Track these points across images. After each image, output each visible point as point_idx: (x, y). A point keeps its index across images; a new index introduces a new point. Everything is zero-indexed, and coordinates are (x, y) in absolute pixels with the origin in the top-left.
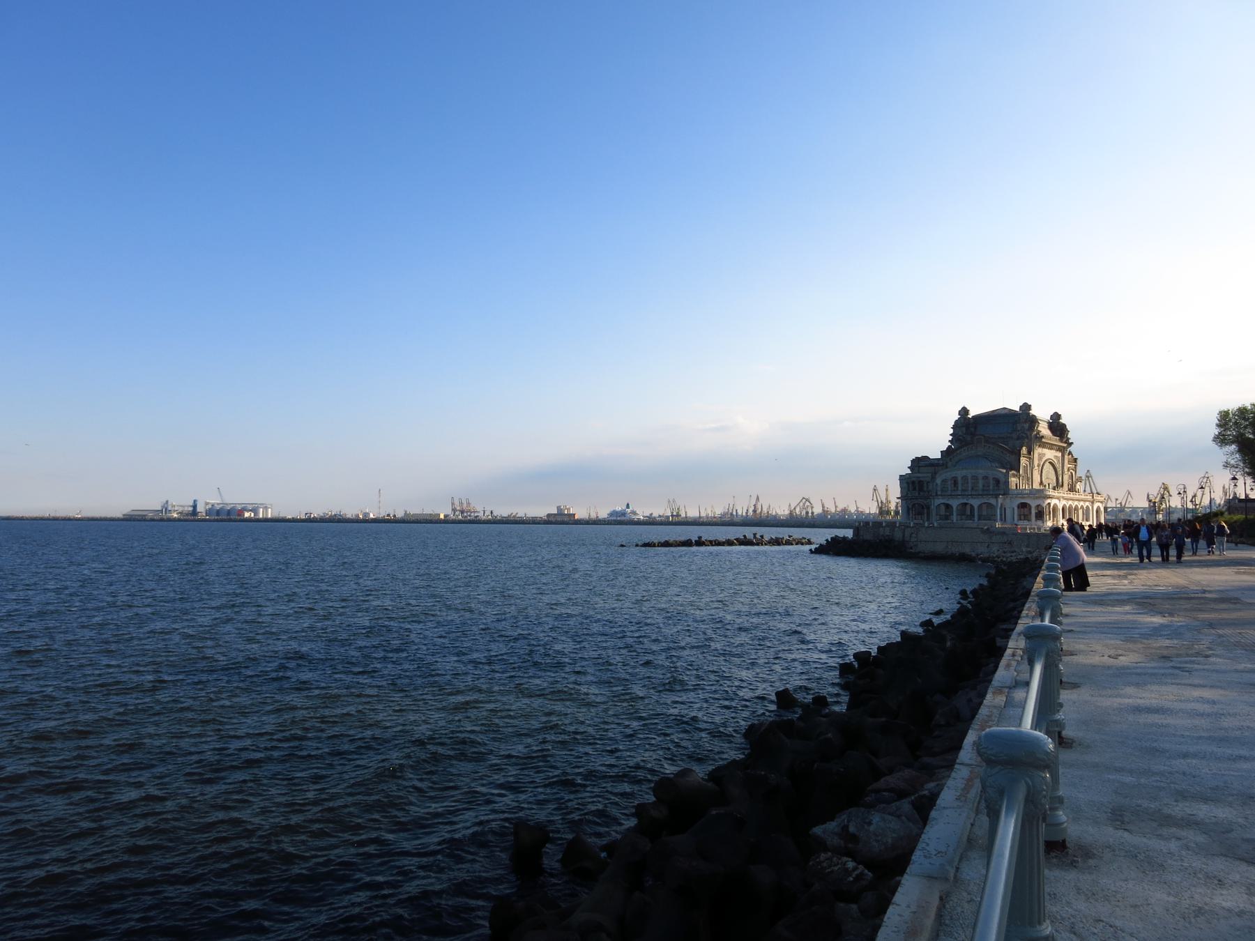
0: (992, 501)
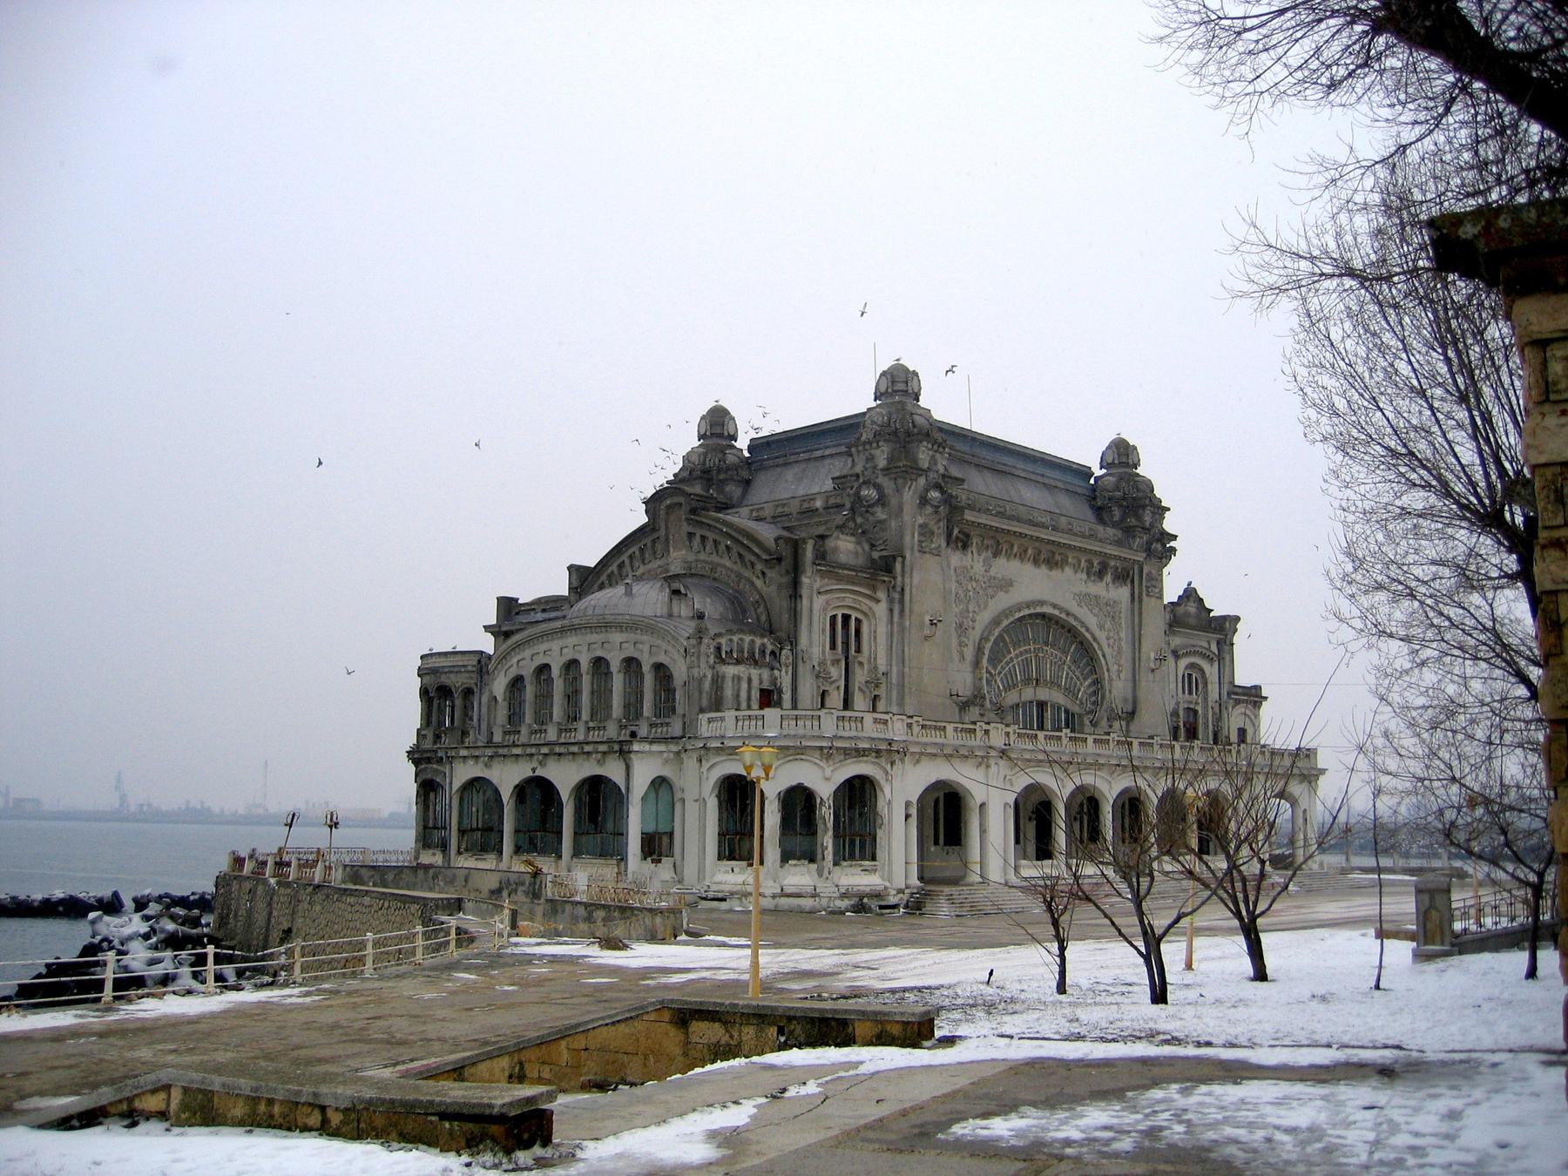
0: (613, 770)
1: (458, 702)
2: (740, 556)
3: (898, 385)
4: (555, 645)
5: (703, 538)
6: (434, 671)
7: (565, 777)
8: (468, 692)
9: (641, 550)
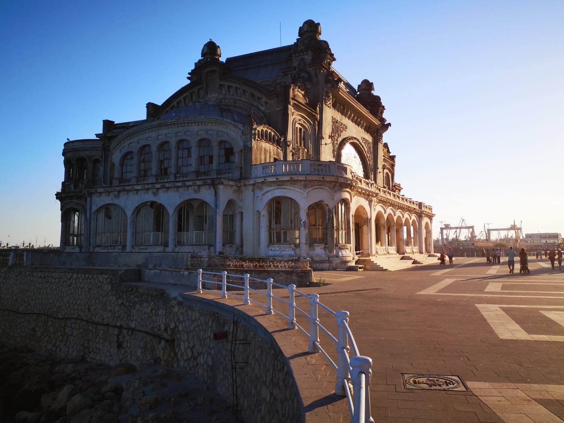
0: (206, 195)
1: (90, 165)
2: (252, 95)
4: (154, 134)
5: (229, 87)
6: (75, 150)
7: (170, 200)
8: (96, 161)
9: (191, 94)
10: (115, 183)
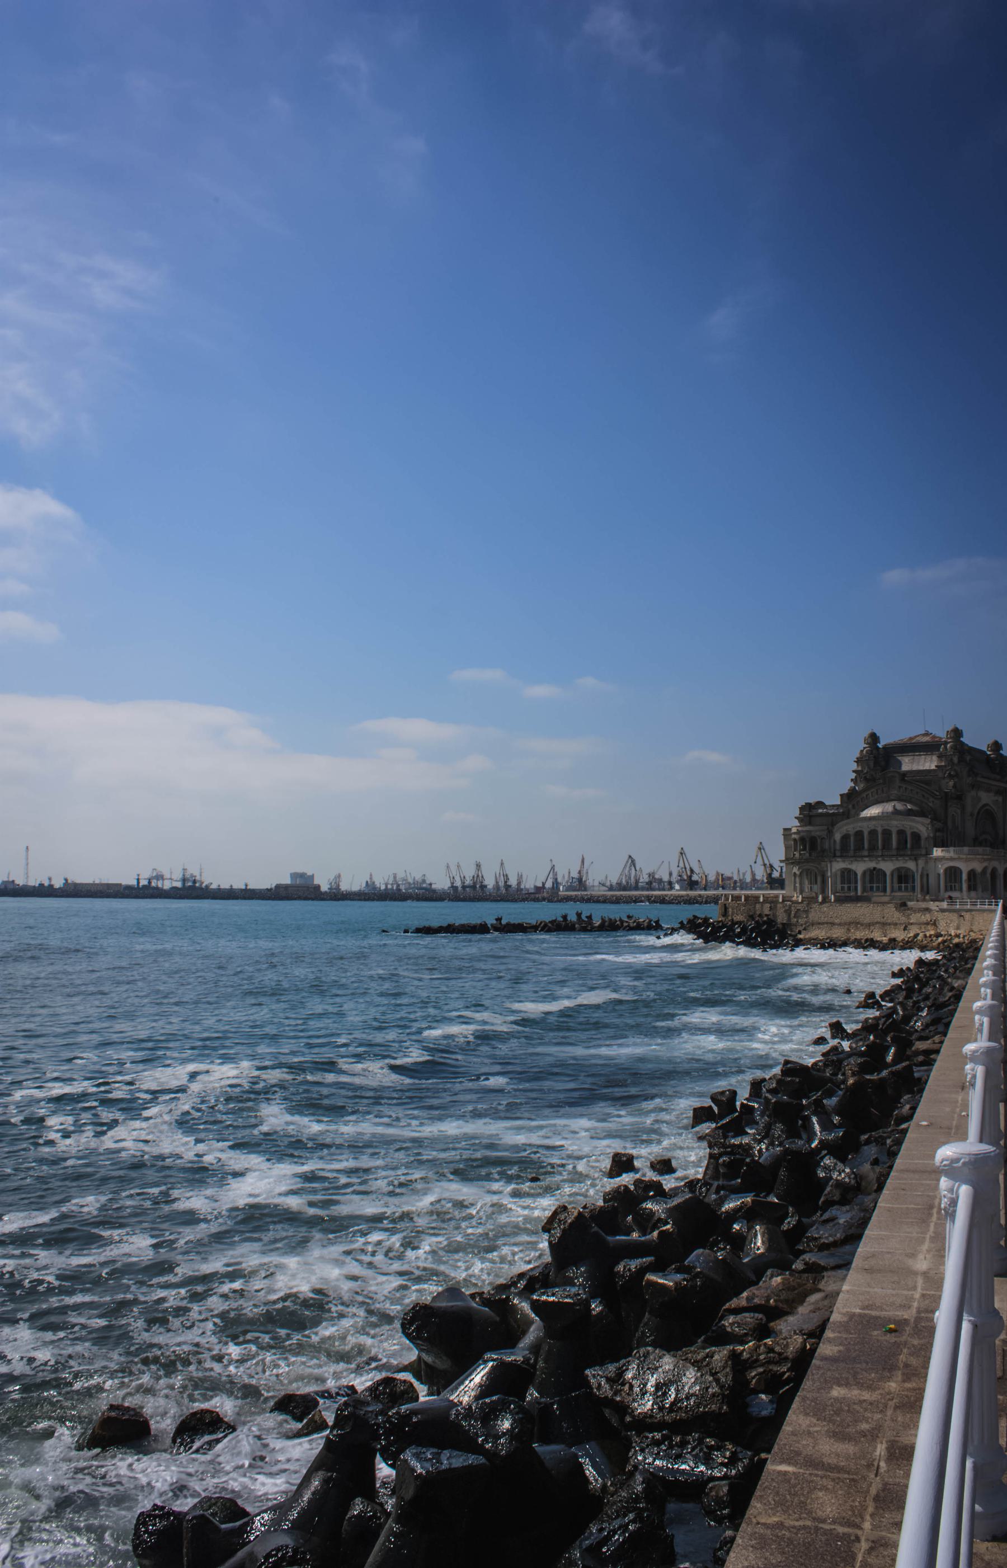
0: (911, 865)
3: (957, 733)
4: (865, 824)
10: (838, 854)
